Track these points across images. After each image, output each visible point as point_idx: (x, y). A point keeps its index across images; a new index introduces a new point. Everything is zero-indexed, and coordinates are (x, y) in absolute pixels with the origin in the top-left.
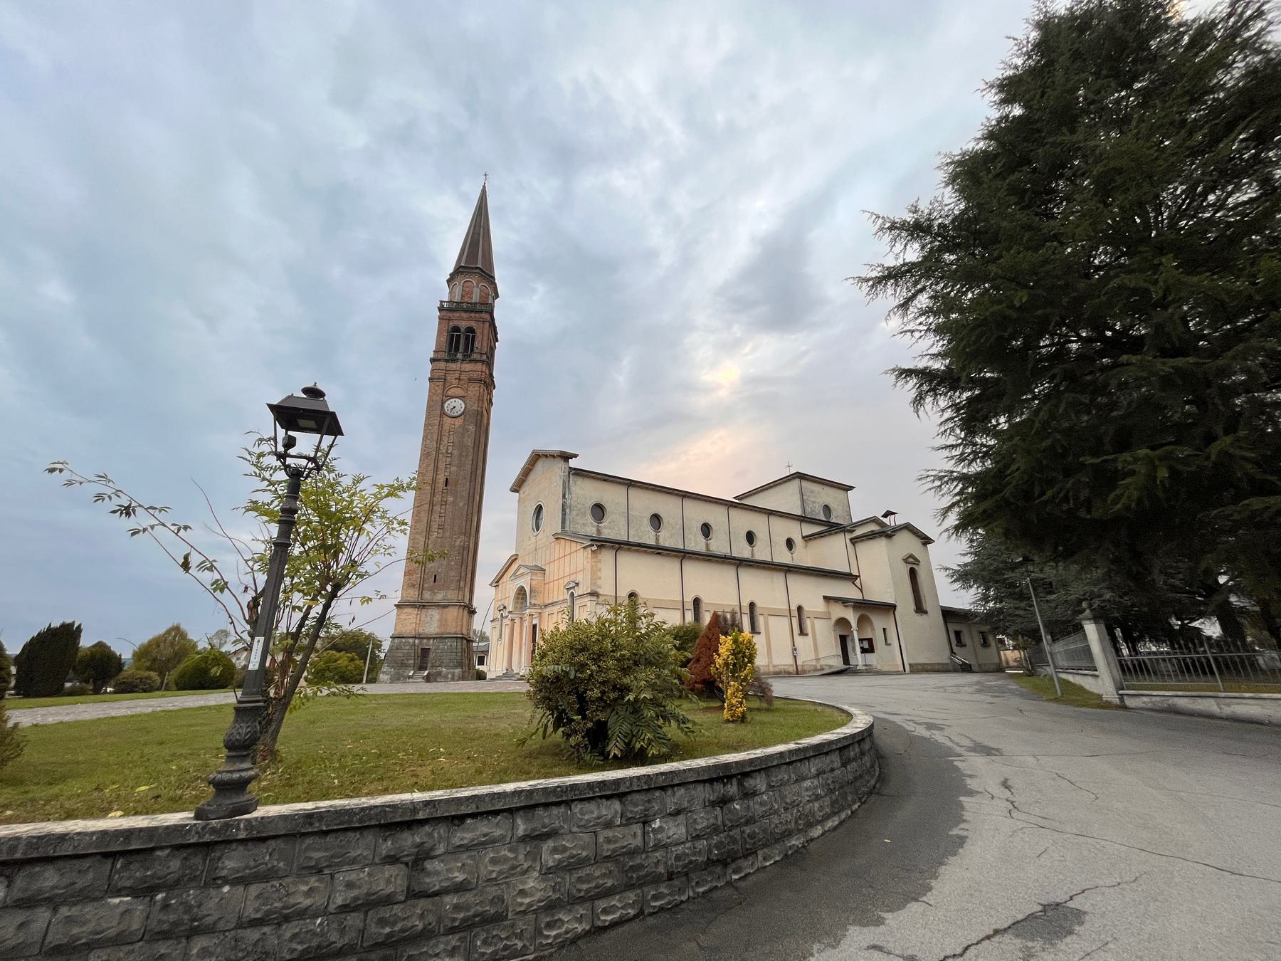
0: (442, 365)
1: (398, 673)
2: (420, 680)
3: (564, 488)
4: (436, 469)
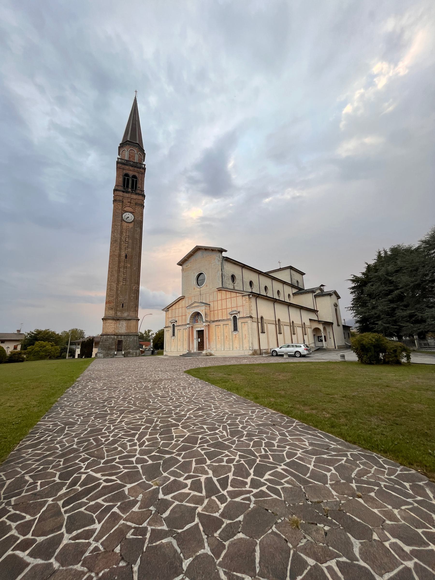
0: (121, 193)
1: (107, 353)
2: (122, 356)
4: (120, 249)
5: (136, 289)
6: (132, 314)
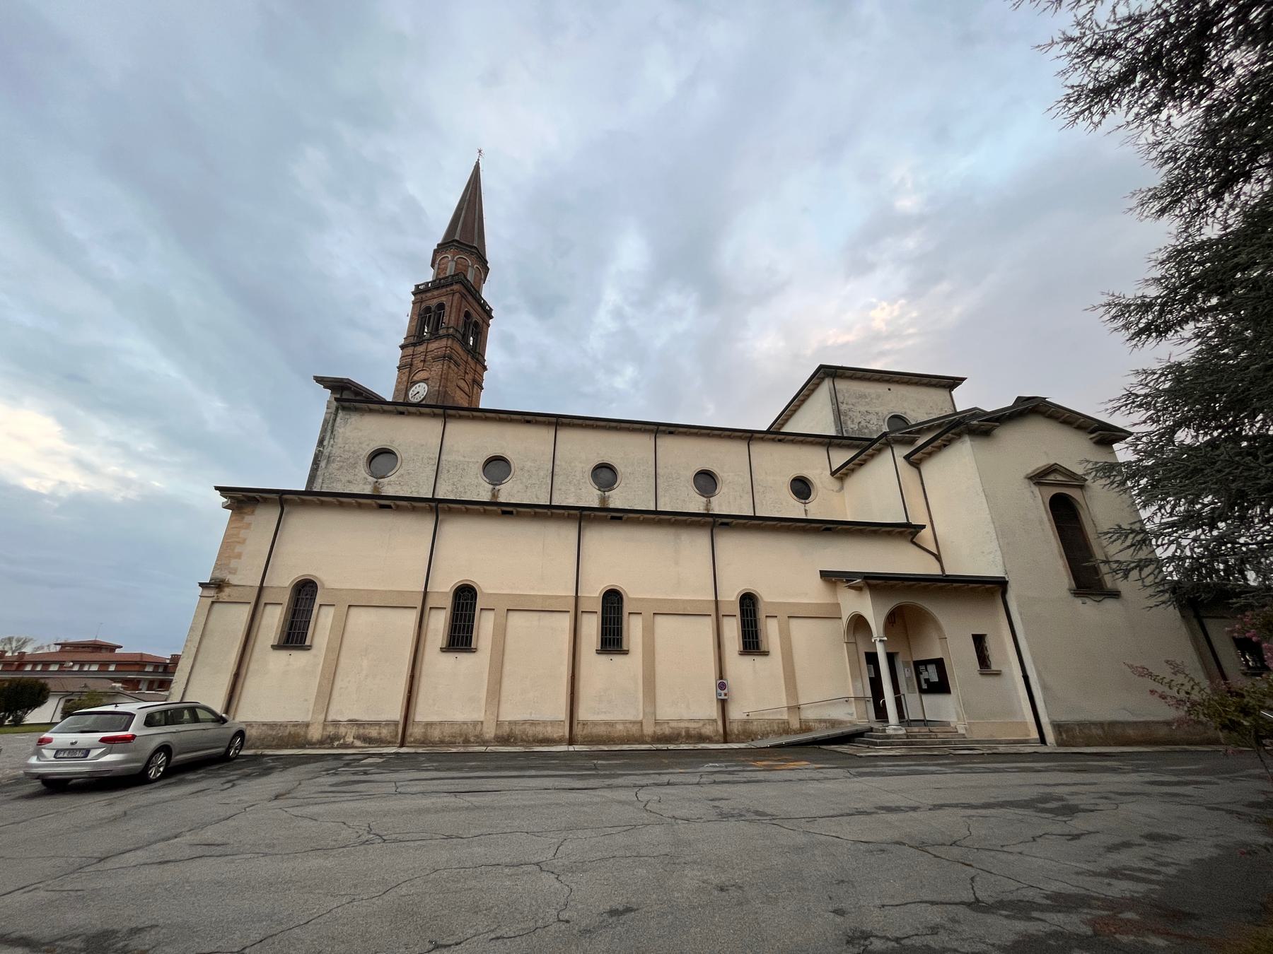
0: (410, 350)
3: (324, 430)
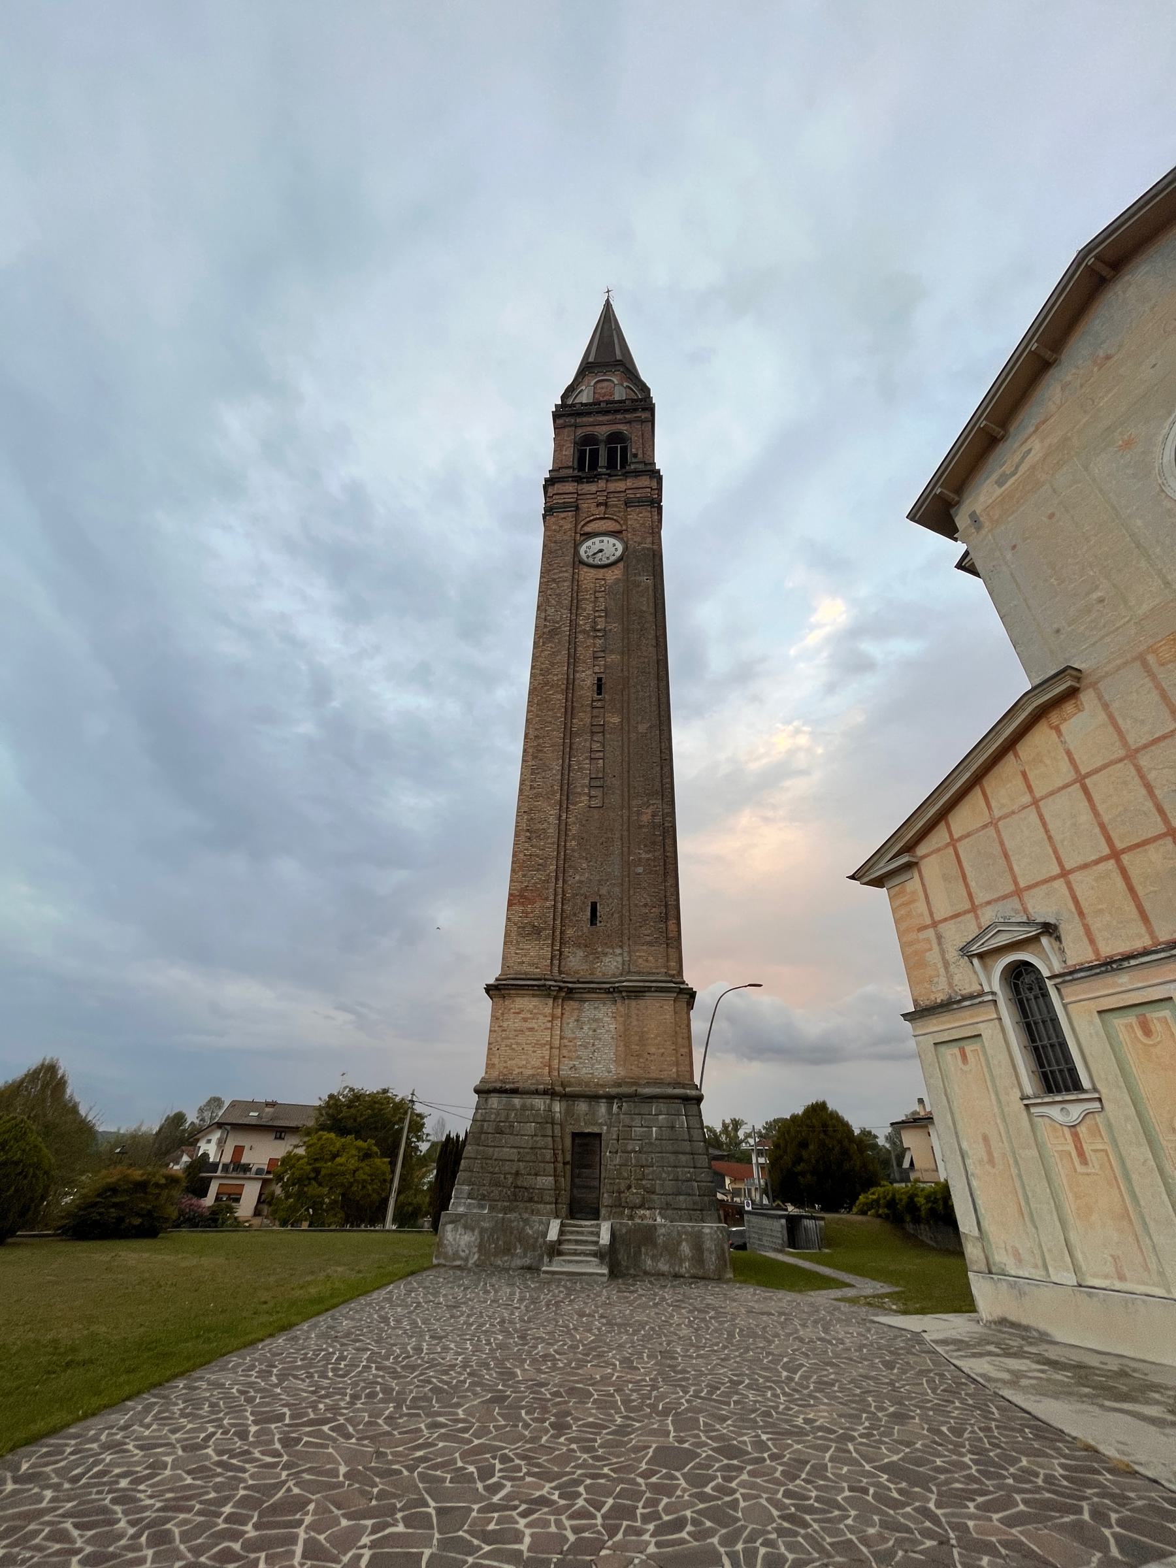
0: (570, 487)
4: (573, 660)
5: (658, 820)
6: (648, 960)
